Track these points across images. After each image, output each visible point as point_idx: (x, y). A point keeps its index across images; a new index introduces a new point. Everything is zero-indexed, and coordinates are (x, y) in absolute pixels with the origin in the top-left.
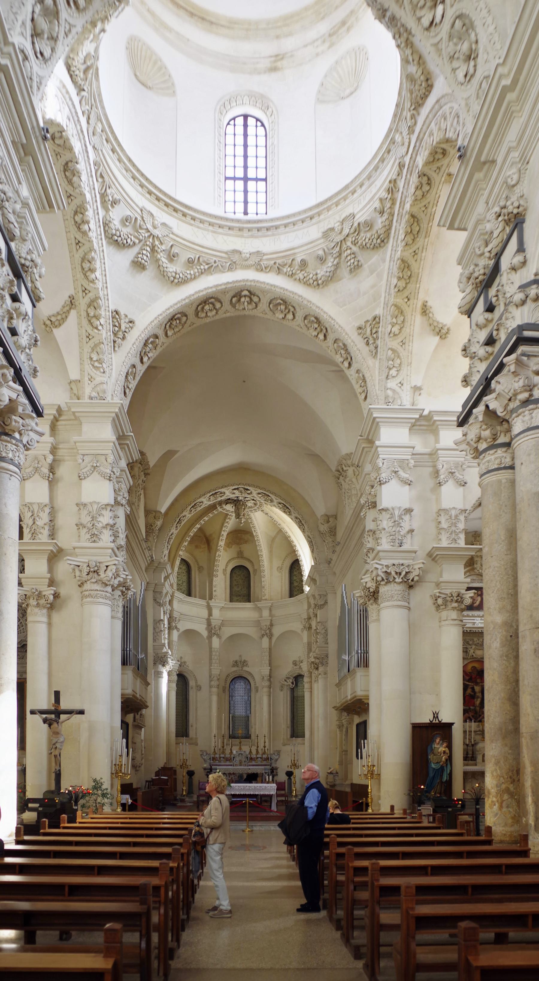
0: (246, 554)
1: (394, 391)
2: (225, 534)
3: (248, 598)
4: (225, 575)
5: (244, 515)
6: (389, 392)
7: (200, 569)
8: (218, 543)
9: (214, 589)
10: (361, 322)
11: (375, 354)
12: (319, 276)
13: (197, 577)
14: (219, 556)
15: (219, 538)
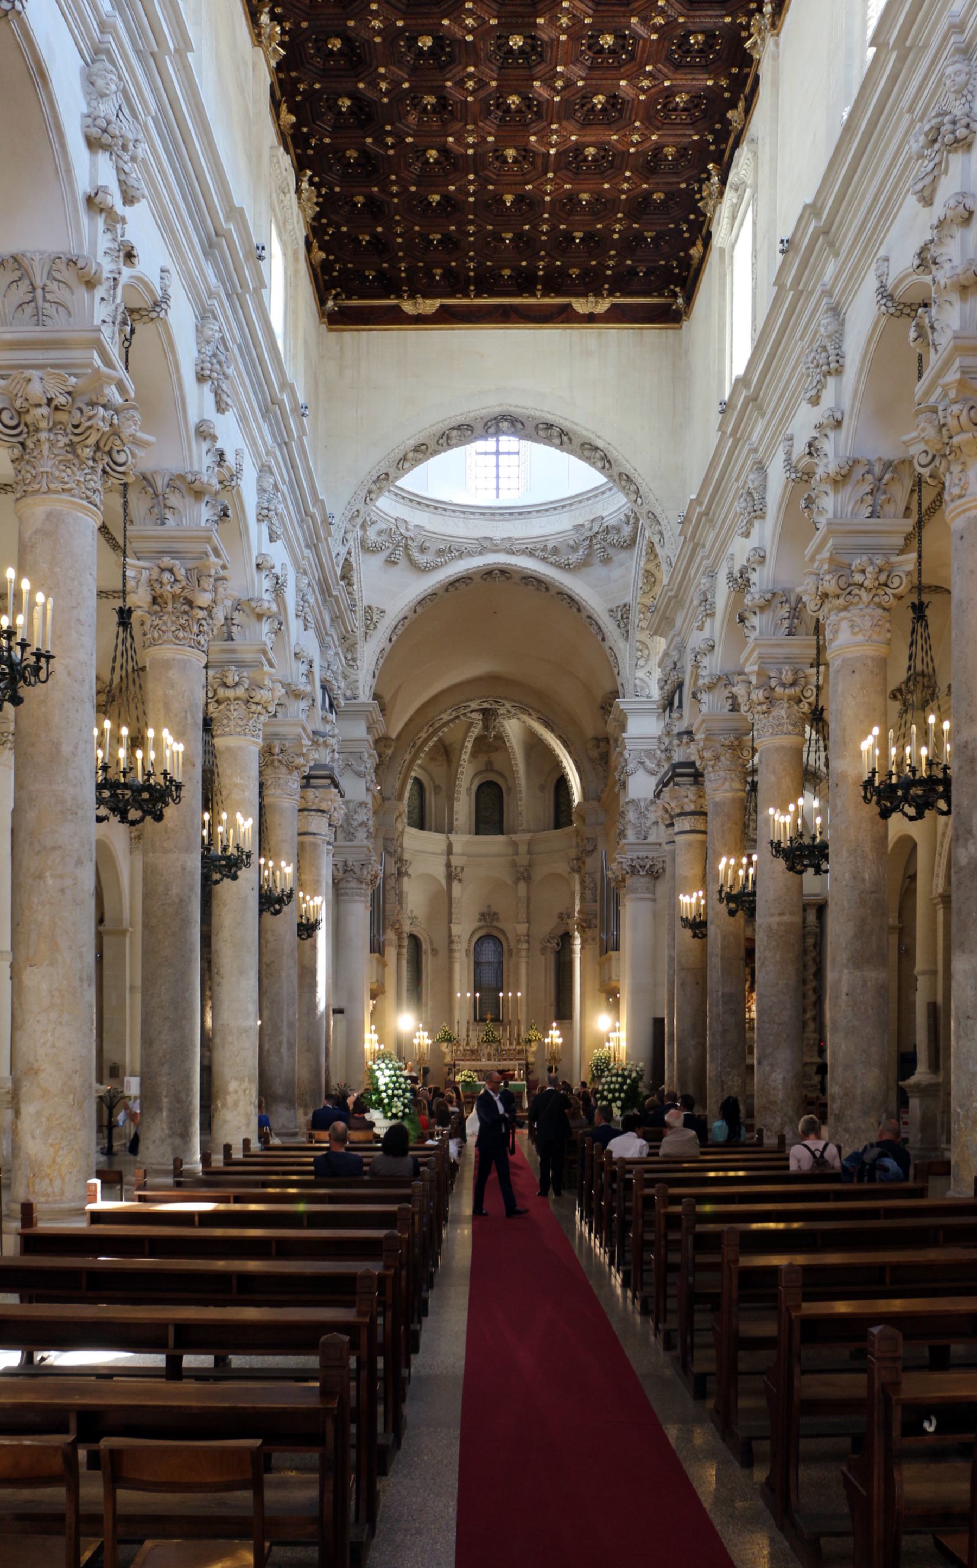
0: (497, 766)
1: (642, 680)
2: (469, 745)
3: (499, 829)
4: (469, 796)
5: (494, 727)
6: (637, 682)
7: (437, 789)
8: (460, 757)
9: (455, 817)
10: (614, 607)
11: (627, 639)
12: (571, 561)
13: (433, 800)
14: (462, 773)
15: (461, 751)
